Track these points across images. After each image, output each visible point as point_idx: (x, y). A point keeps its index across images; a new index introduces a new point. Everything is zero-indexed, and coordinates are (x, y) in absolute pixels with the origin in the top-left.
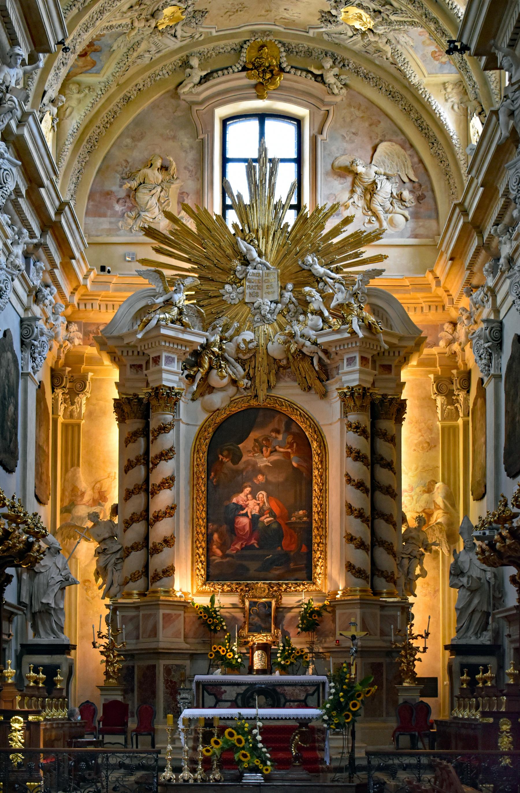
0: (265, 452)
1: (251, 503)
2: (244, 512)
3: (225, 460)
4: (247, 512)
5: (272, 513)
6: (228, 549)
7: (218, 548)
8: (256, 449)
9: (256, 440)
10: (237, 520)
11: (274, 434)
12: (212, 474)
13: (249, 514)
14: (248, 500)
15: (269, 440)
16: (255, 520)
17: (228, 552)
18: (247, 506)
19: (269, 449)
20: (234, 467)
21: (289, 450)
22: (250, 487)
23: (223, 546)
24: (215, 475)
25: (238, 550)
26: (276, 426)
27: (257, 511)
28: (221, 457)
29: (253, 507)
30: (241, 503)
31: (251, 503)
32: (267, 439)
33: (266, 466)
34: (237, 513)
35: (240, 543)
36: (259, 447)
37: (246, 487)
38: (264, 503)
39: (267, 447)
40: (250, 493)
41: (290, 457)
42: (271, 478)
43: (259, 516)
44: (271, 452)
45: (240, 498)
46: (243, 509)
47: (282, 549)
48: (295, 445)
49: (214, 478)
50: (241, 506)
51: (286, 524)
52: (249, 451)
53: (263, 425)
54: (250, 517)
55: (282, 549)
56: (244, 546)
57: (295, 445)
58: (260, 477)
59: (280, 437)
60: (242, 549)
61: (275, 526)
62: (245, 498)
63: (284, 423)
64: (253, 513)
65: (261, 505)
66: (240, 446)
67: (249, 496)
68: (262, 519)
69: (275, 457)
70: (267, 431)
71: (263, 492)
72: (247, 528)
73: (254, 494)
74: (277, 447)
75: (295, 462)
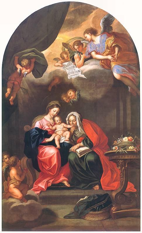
0: (76, 60)
1: (60, 128)
2: (51, 139)
3: (25, 71)
4: (54, 140)
5: (87, 141)
6: (29, 189)
7: (16, 187)
8: (65, 56)
9: (65, 45)
10: (41, 152)
11: (88, 36)
12: (9, 90)
13: (57, 143)
14: (55, 124)
15: (82, 44)
16: (64, 150)
17: (30, 192)
18: (54, 131)
19: (83, 57)
20: (37, 80)
21: (109, 57)
22: (57, 106)
23: (23, 185)
24: (12, 91)
25: (42, 190)
26: (92, 26)
27: (67, 138)
28: (19, 67)
29: (61, 134)
30: (46, 127)
31: (60, 128)
32: (79, 43)
33: (79, 78)
34: (40, 142)
35: (45, 180)
36: (70, 53)
37: (52, 107)
38: (77, 127)
39: (80, 53)
40: (58, 114)
41: (110, 67)
42: (85, 95)
43: (70, 146)
44: (86, 60)
45: (43, 122)
46: (49, 136)
47: (101, 187)
48: (117, 49)
49: (10, 95)
50: (46, 132)
51: (106, 155)
52: (56, 59)
53: (73, 24)
54: (58, 146)
55: (101, 187)
56: (50, 184)
57: (117, 49)
58: (71, 93)
59: (97, 40)
60: (49, 188)
61: (91, 158)
62: (52, 121)
63: (102, 21)
64: (62, 141)
65: (72, 130)
66: (45, 52)
67: (57, 119)
68: (73, 149)
69: (90, 67)
70: (78, 33)
71: (75, 113)
72: (55, 161)
73: (63, 115)
74: (93, 54)
75: (118, 71)
